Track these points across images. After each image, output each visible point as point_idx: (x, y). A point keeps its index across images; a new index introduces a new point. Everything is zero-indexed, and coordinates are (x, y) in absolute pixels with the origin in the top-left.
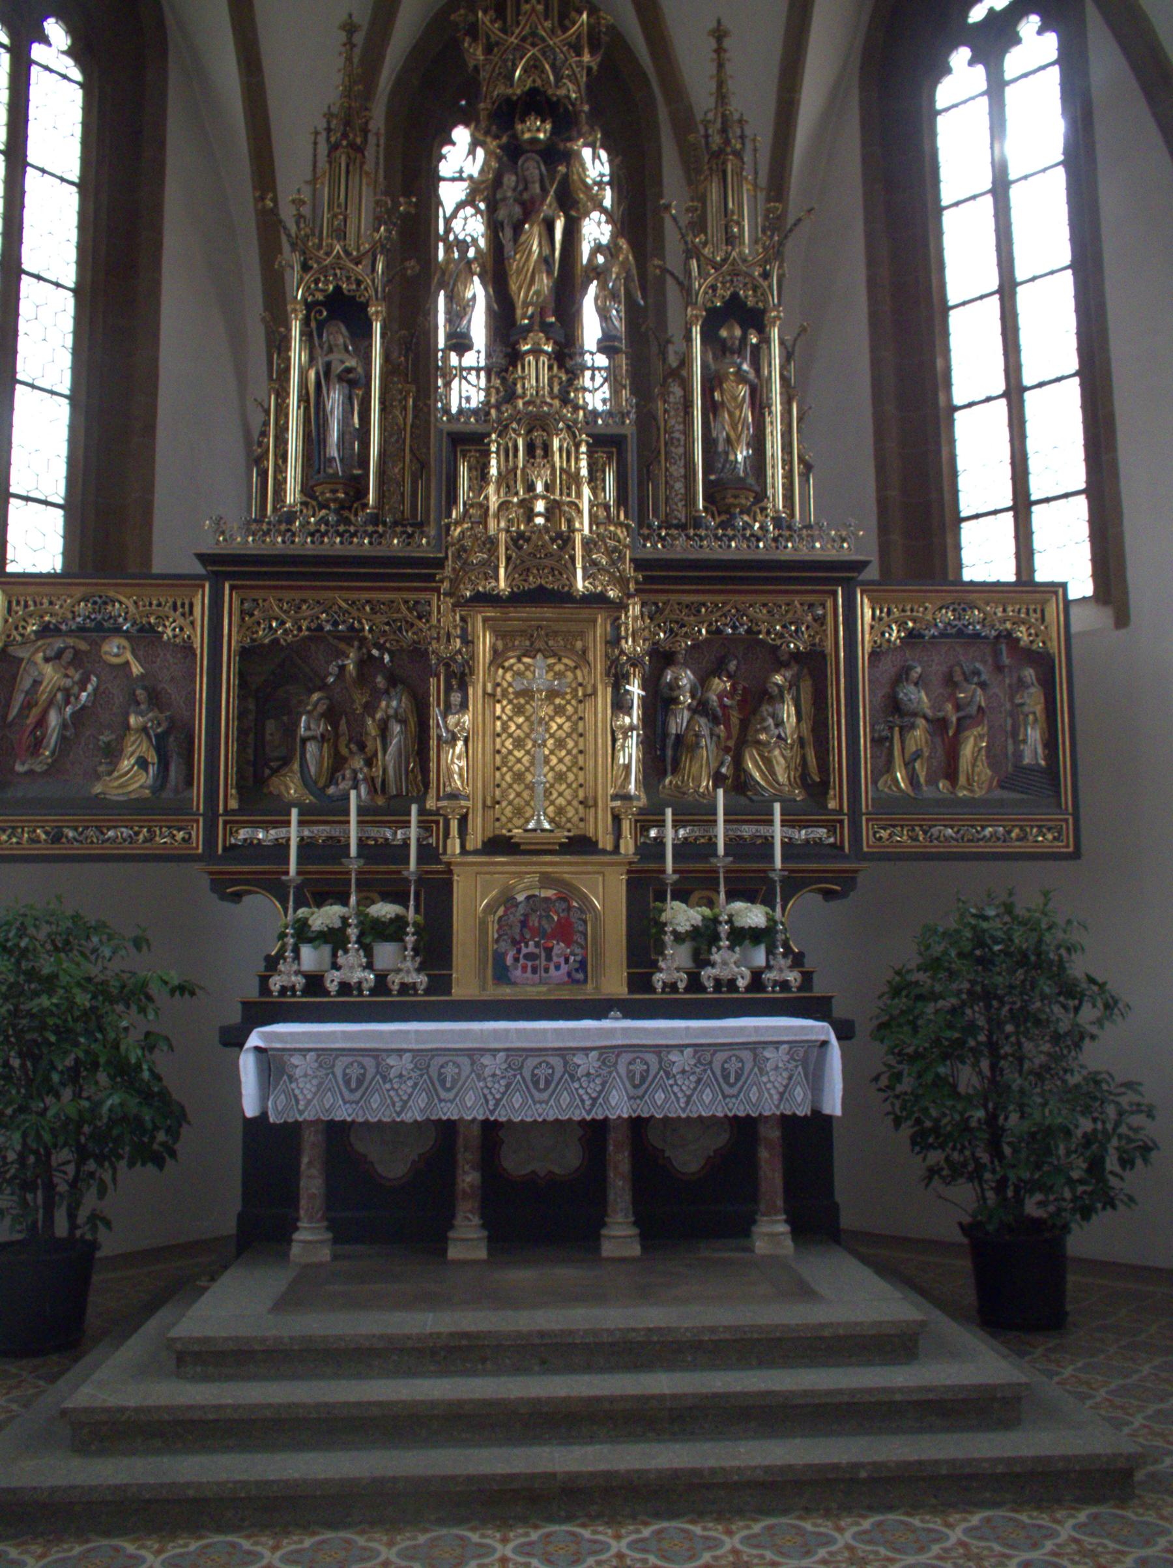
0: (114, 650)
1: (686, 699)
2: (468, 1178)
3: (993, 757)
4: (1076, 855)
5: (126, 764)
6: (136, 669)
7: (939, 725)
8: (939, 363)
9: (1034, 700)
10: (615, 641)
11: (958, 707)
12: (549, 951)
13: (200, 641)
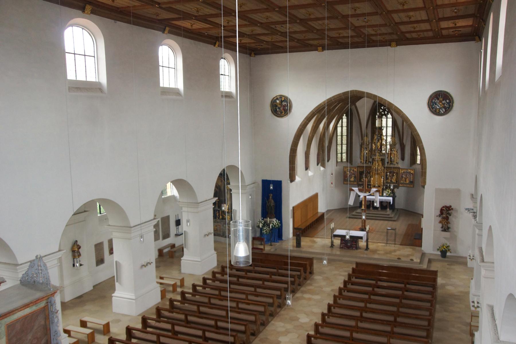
0: (352, 171)
1: (388, 175)
2: (371, 205)
3: (409, 180)
4: (414, 187)
5: (352, 178)
6: (353, 172)
7: (405, 178)
9: (412, 176)
10: (381, 175)
11: (407, 177)
13: (357, 171)
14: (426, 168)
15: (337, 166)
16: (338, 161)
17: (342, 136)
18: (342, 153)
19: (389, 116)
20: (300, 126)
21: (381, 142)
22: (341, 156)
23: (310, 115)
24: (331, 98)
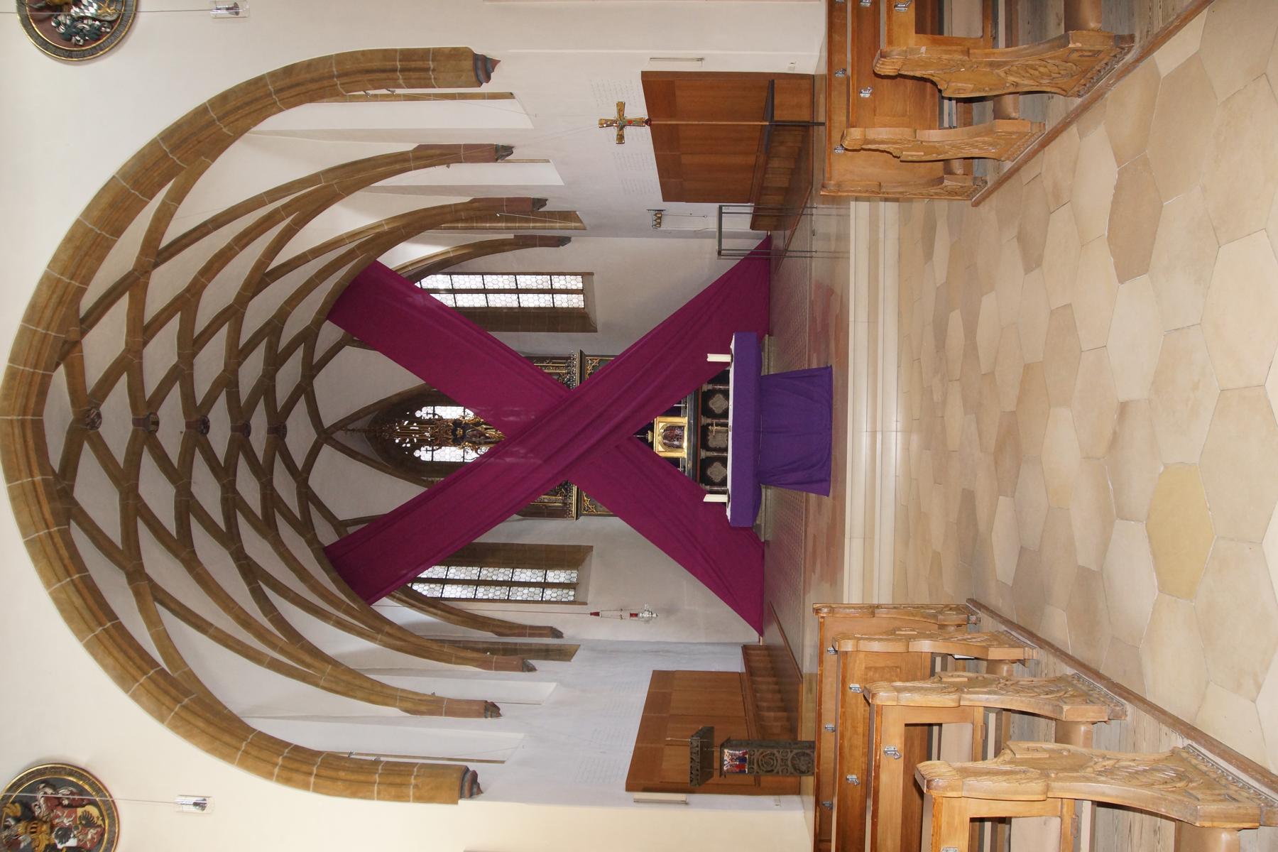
8: (505, 311)
12: (677, 435)
14: (387, 54)
15: (585, 604)
16: (572, 598)
17: (478, 583)
18: (545, 585)
19: (425, 413)
20: (161, 719)
21: (484, 426)
22: (555, 590)
23: (110, 661)
24: (30, 544)
